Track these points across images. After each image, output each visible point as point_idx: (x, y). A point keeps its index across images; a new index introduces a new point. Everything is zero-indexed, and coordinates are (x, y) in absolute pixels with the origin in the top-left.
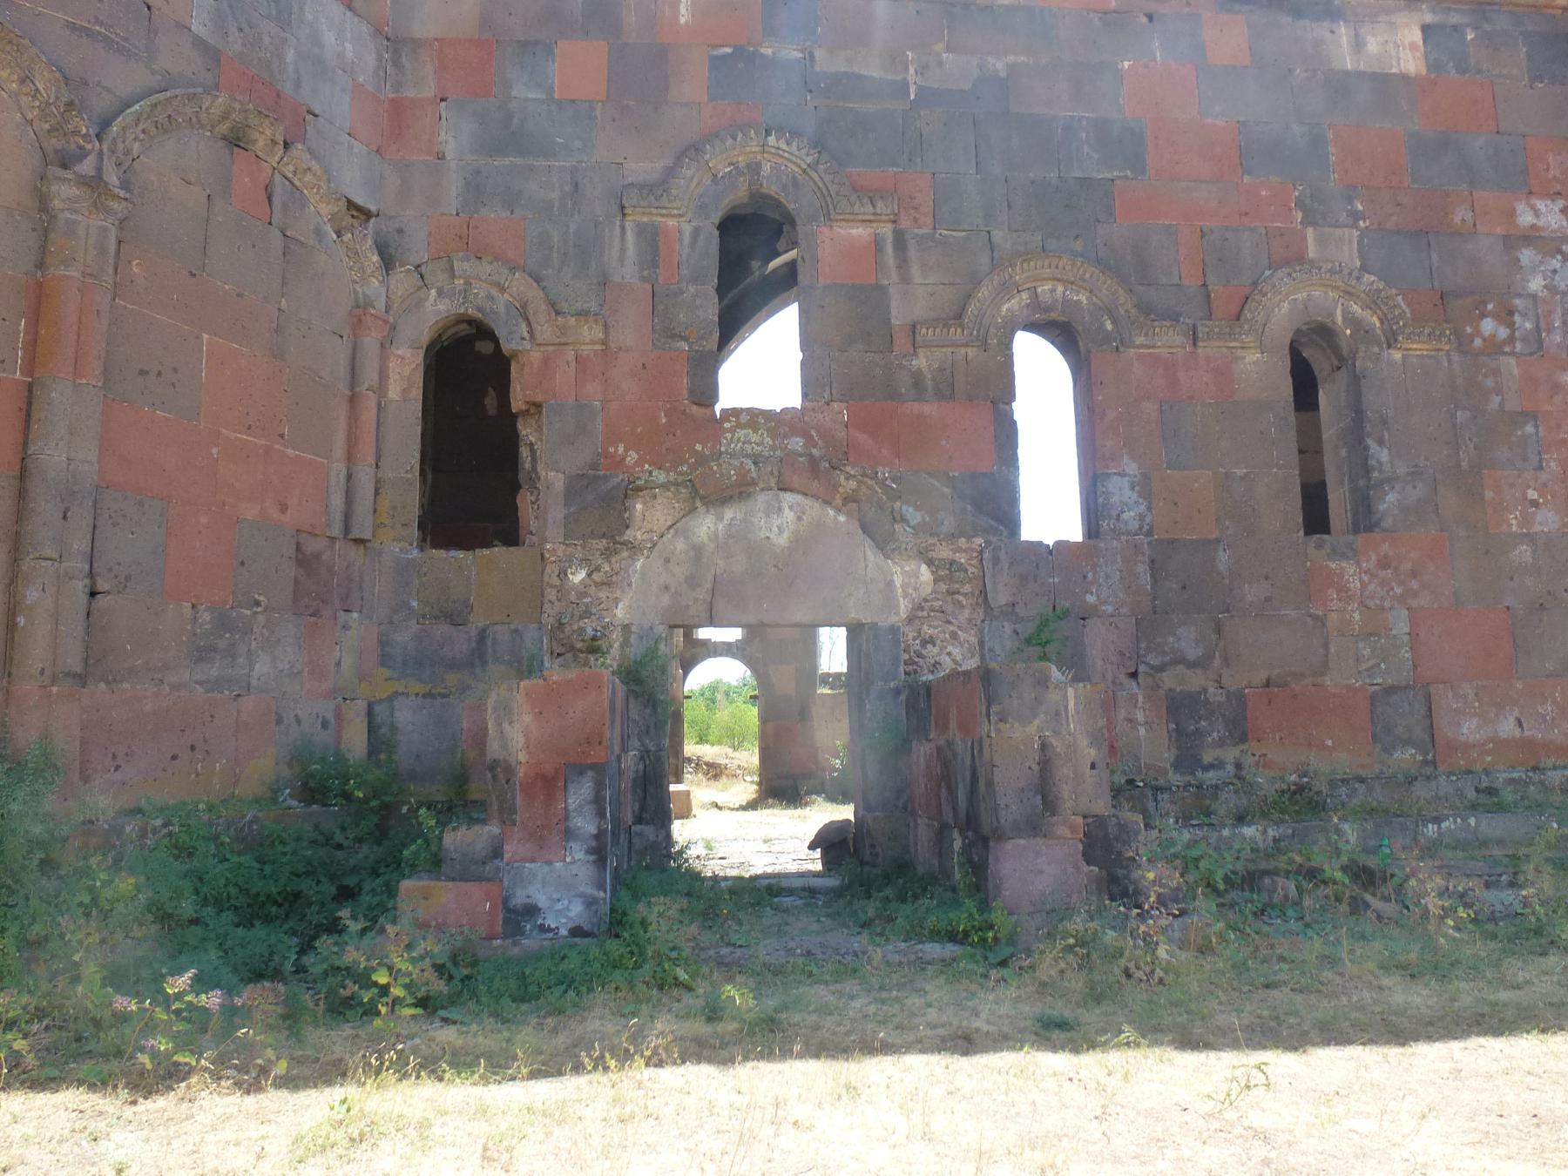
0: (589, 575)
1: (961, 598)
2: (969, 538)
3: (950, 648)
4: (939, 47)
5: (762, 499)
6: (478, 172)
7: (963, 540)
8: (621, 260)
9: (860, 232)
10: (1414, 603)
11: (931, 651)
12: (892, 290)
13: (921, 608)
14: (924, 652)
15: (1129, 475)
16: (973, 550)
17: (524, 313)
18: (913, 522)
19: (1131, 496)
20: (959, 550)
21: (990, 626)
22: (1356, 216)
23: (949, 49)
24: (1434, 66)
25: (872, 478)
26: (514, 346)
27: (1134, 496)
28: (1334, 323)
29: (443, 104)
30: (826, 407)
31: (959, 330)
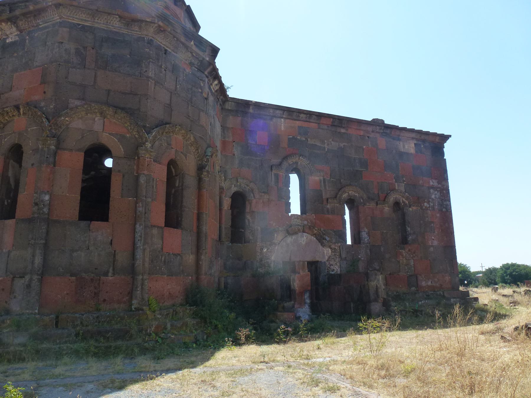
0: (267, 250)
2: (338, 243)
3: (335, 267)
4: (331, 140)
5: (300, 234)
7: (337, 244)
8: (271, 181)
9: (317, 178)
10: (414, 258)
11: (332, 267)
14: (331, 267)
17: (252, 190)
18: (328, 240)
19: (366, 236)
22: (404, 181)
23: (333, 141)
24: (416, 152)
27: (367, 236)
28: (400, 202)
29: (234, 143)
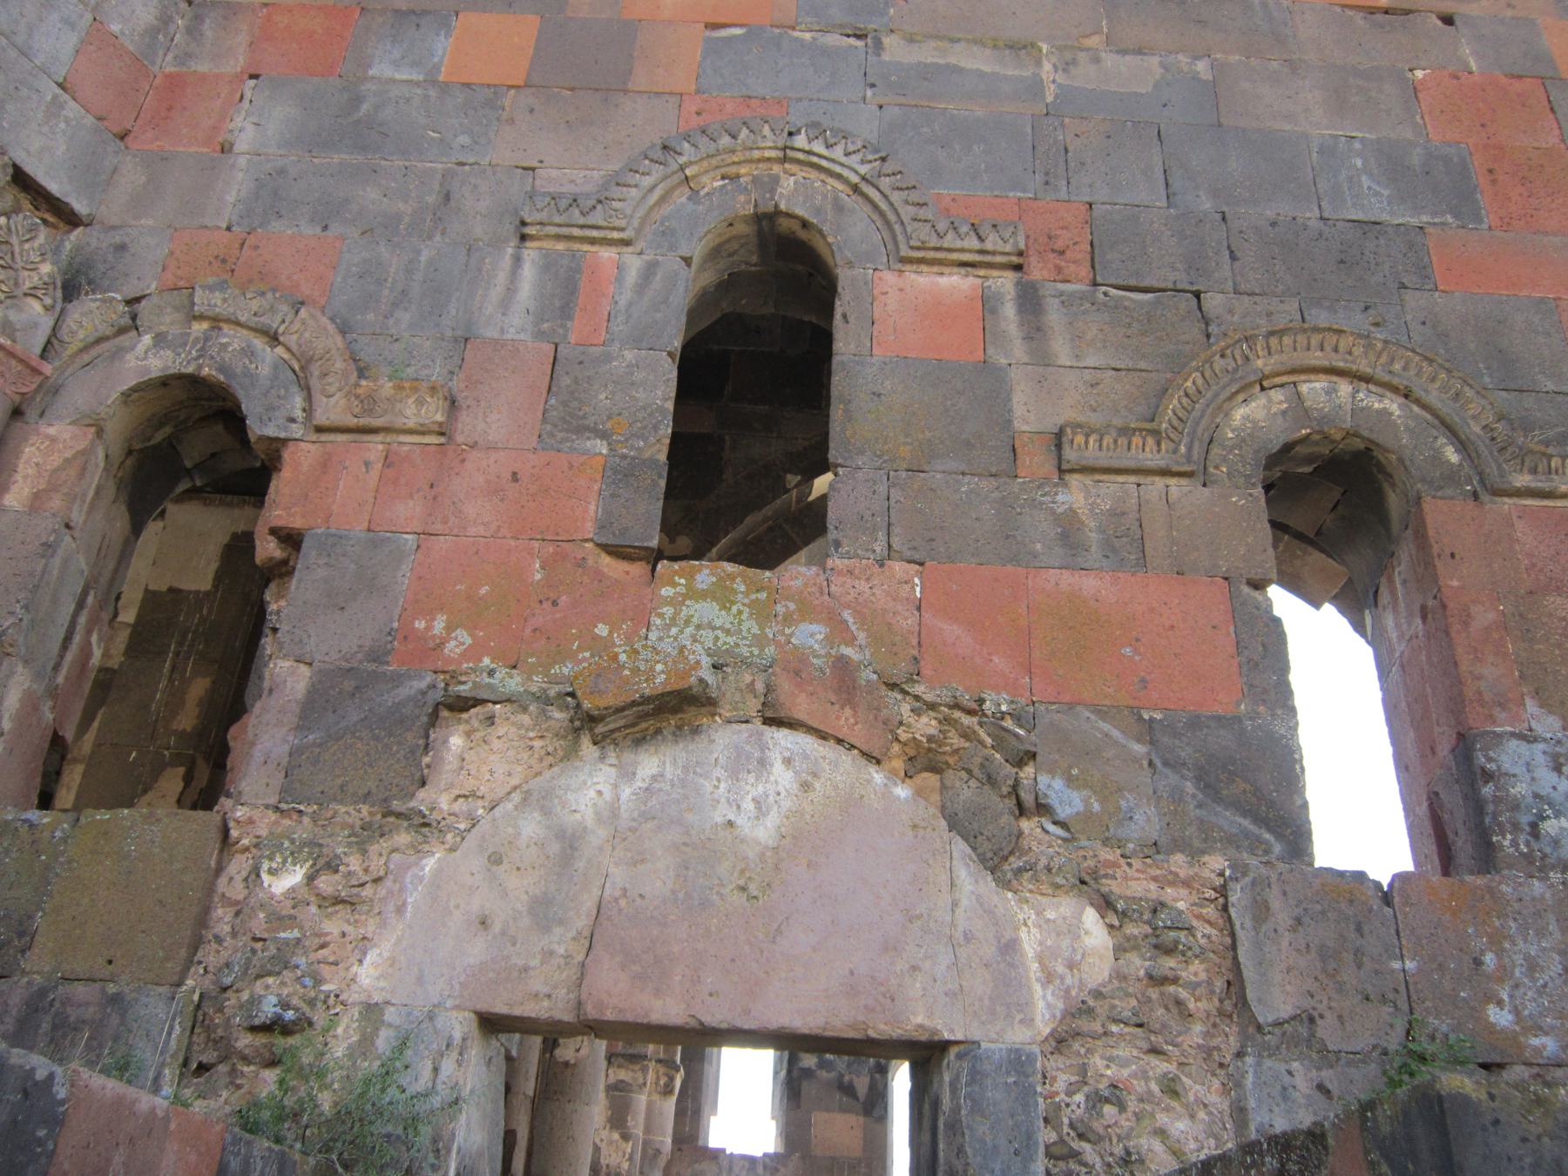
0: (310, 879)
1: (1183, 994)
2: (1195, 854)
5: (722, 739)
6: (282, 172)
7: (1179, 858)
8: (506, 304)
12: (1014, 374)
15: (1545, 740)
18: (1063, 812)
20: (1175, 881)
21: (1259, 1064)
25: (970, 712)
26: (271, 431)
29: (252, 82)
30: (876, 569)
31: (1150, 441)
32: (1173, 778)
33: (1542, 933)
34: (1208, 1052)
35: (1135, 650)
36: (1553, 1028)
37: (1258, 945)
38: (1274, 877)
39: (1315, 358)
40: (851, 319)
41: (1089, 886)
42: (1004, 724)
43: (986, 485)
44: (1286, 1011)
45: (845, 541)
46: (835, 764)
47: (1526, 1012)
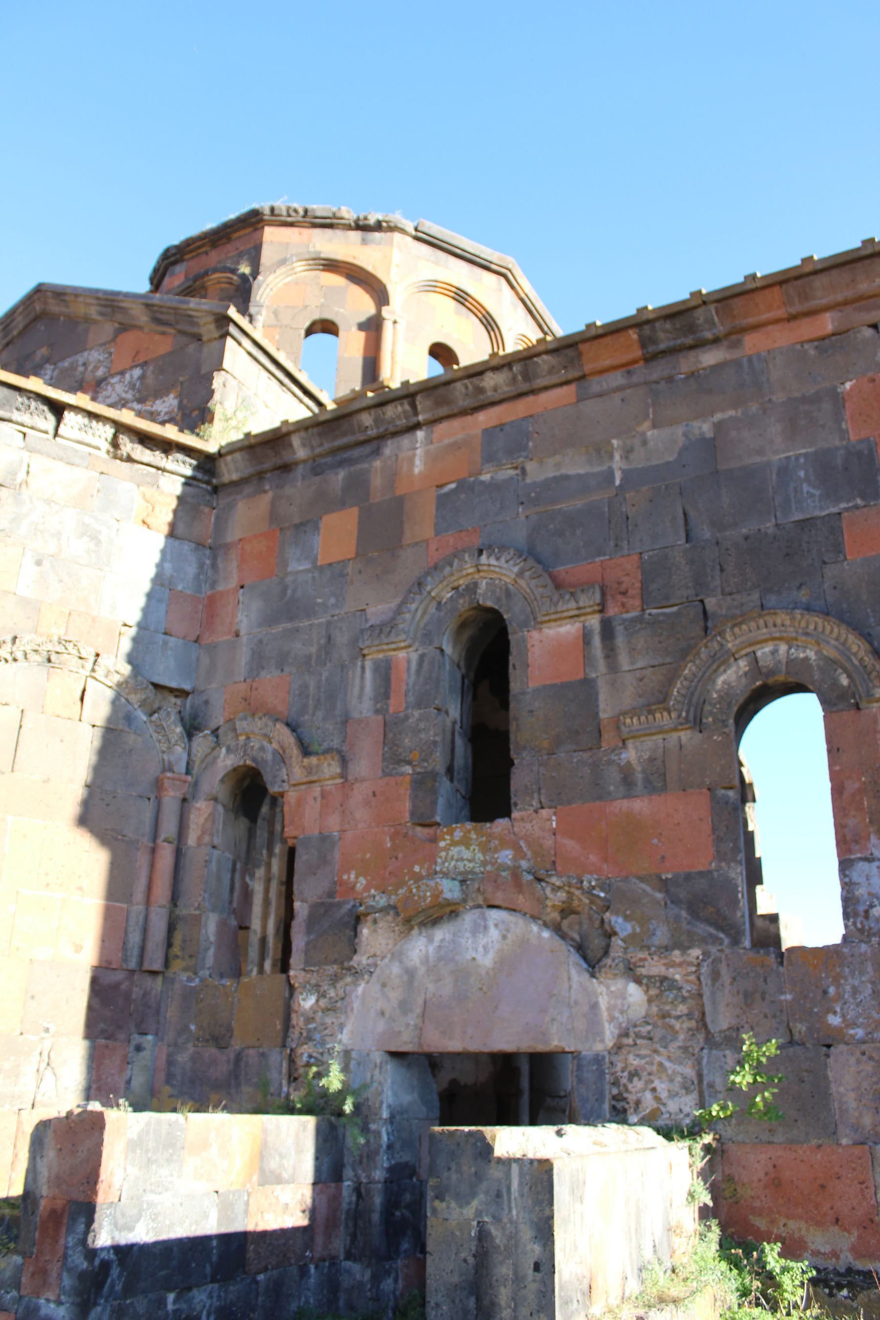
0: (317, 1001)
2: (684, 949)
4: (647, 424)
5: (469, 918)
7: (677, 952)
8: (360, 697)
13: (627, 1035)
16: (690, 964)
20: (673, 965)
21: (710, 1053)
23: (654, 426)
25: (578, 888)
29: (241, 591)
30: (534, 815)
31: (665, 714)
32: (676, 910)
33: (862, 973)
34: (685, 1049)
35: (659, 840)
36: (862, 1024)
37: (713, 994)
38: (723, 957)
39: (764, 634)
40: (517, 667)
41: (631, 972)
42: (594, 892)
43: (586, 755)
44: (725, 1026)
45: (519, 802)
46: (516, 924)
47: (849, 1017)
